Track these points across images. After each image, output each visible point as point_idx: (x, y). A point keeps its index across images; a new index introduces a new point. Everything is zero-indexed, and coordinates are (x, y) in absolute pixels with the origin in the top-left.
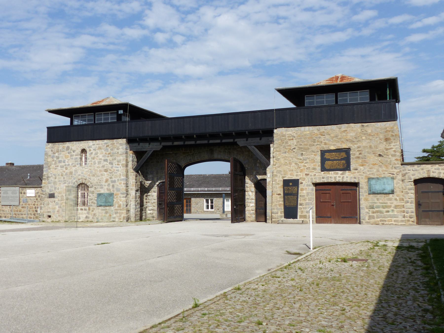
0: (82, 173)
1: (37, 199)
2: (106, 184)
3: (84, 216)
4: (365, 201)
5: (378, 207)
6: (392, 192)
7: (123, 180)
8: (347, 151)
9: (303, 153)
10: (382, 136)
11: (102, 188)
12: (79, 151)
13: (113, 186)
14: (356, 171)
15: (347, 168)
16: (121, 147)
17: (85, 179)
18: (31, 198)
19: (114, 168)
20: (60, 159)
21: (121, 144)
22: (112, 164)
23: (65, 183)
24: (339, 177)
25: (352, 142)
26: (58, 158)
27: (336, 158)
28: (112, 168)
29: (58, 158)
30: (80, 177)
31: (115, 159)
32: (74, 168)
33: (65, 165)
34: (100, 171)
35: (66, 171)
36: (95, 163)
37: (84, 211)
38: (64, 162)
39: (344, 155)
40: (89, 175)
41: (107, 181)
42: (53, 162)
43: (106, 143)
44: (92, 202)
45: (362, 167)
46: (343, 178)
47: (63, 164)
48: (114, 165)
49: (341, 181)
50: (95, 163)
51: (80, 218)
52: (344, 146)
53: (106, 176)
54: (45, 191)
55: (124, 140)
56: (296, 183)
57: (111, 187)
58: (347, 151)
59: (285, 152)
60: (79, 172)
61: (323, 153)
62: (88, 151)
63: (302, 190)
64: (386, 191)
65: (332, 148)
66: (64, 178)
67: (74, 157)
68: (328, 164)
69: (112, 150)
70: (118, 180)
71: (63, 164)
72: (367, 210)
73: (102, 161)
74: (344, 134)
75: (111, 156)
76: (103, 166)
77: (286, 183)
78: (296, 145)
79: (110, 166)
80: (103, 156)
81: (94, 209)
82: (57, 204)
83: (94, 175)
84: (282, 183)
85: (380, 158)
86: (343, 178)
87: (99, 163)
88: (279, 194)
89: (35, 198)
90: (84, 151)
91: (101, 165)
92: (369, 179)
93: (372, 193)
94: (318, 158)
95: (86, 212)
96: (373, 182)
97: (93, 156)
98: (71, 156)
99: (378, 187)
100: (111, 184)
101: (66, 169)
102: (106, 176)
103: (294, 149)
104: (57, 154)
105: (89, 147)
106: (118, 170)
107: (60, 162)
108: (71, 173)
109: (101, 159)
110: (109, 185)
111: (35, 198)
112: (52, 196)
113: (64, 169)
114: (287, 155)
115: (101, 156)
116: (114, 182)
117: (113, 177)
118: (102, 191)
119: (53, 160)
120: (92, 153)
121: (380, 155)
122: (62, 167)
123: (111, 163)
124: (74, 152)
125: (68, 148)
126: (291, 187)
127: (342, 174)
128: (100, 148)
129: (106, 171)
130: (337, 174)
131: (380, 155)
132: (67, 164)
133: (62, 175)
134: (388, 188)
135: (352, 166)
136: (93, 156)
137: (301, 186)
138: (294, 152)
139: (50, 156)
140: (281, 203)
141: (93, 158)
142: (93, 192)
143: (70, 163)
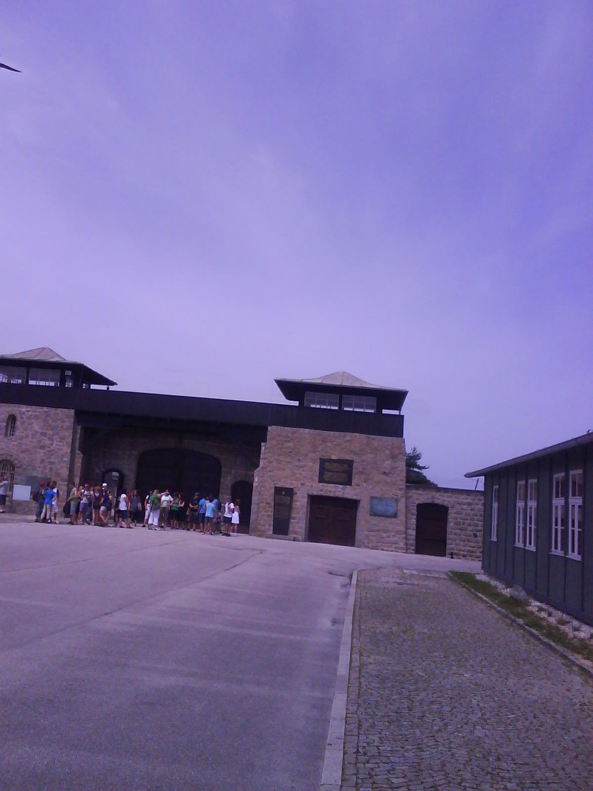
4: (364, 521)
6: (395, 516)
8: (350, 463)
9: (301, 458)
10: (388, 452)
13: (51, 469)
14: (358, 487)
15: (348, 482)
16: (66, 420)
19: (54, 445)
21: (68, 416)
22: (52, 440)
24: (340, 491)
25: (356, 454)
27: (337, 470)
28: (52, 444)
31: (57, 434)
39: (346, 466)
45: (364, 484)
48: (55, 443)
49: (341, 496)
52: (348, 457)
58: (350, 463)
59: (280, 455)
61: (323, 461)
63: (297, 501)
65: (334, 457)
68: (327, 475)
69: (54, 421)
72: (367, 533)
74: (348, 444)
75: (52, 430)
78: (293, 449)
84: (273, 491)
85: (384, 477)
86: (344, 493)
88: (268, 503)
92: (372, 498)
93: (374, 514)
94: (317, 466)
99: (380, 508)
103: (291, 452)
114: (281, 458)
116: (52, 463)
121: (385, 473)
123: (51, 439)
126: (284, 496)
130: (338, 487)
131: (385, 473)
134: (391, 510)
135: (354, 481)
137: (295, 498)
138: (290, 456)
140: (269, 513)
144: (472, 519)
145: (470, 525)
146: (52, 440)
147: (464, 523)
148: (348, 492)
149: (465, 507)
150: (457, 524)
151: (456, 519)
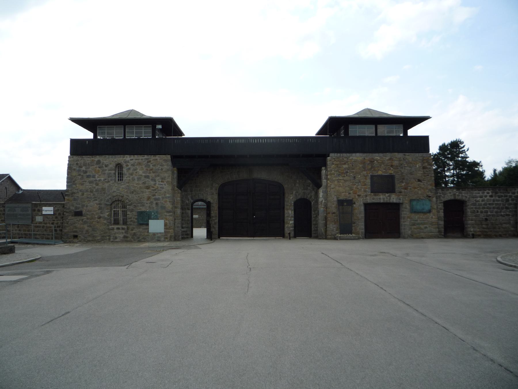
0: (118, 189)
1: (56, 218)
2: (149, 202)
3: (122, 236)
5: (418, 224)
6: (430, 211)
7: (169, 197)
11: (143, 206)
12: (112, 166)
13: (157, 204)
17: (122, 197)
18: (49, 217)
19: (157, 185)
20: (88, 174)
21: (165, 161)
22: (155, 181)
23: (96, 200)
26: (86, 172)
28: (155, 184)
29: (86, 172)
30: (115, 194)
31: (158, 176)
32: (107, 185)
33: (96, 180)
34: (141, 188)
35: (97, 187)
36: (133, 180)
37: (121, 231)
38: (94, 177)
40: (127, 192)
41: (149, 198)
42: (80, 177)
43: (147, 159)
44: (131, 221)
46: (390, 199)
47: (92, 179)
48: (157, 182)
49: (388, 202)
50: (133, 180)
51: (116, 238)
53: (147, 193)
54: (69, 208)
55: (169, 157)
56: (350, 202)
57: (154, 205)
60: (114, 189)
62: (124, 165)
64: (425, 211)
66: (94, 195)
67: (107, 172)
69: (154, 165)
70: (163, 198)
71: (92, 179)
73: (143, 178)
75: (153, 172)
76: (144, 183)
77: (341, 203)
79: (152, 183)
80: (144, 173)
81: (134, 228)
82: (85, 223)
83: (133, 192)
84: (336, 203)
87: (139, 179)
88: (334, 213)
89: (54, 217)
90: (119, 166)
91: (141, 182)
93: (413, 211)
95: (123, 231)
96: (414, 203)
97: (131, 171)
98: (103, 170)
99: (418, 206)
100: (155, 202)
101: (97, 185)
102: (147, 193)
104: (84, 168)
105: (126, 162)
106: (163, 188)
107: (88, 177)
108: (103, 189)
109: (141, 175)
110: (151, 203)
111: (54, 217)
112: (79, 214)
113: (94, 186)
115: (141, 172)
117: (156, 194)
118: (143, 209)
119: (80, 175)
120: (129, 169)
122: (91, 182)
124: (106, 166)
125: (99, 162)
127: (389, 196)
128: (139, 164)
129: (148, 188)
132: (98, 179)
133: (91, 192)
134: (427, 208)
136: (131, 171)
139: (74, 169)
141: (132, 174)
142: (132, 211)
143: (102, 179)
144: (484, 208)
145: (482, 212)
146: (155, 181)
147: (478, 211)
148: (394, 198)
149: (478, 199)
150: (473, 212)
151: (472, 208)
